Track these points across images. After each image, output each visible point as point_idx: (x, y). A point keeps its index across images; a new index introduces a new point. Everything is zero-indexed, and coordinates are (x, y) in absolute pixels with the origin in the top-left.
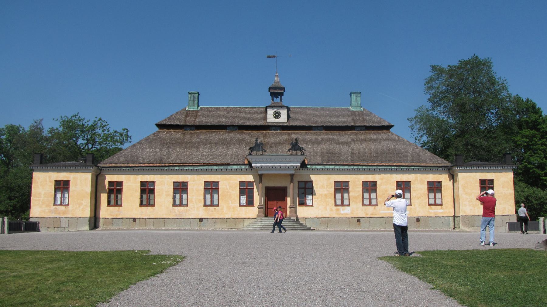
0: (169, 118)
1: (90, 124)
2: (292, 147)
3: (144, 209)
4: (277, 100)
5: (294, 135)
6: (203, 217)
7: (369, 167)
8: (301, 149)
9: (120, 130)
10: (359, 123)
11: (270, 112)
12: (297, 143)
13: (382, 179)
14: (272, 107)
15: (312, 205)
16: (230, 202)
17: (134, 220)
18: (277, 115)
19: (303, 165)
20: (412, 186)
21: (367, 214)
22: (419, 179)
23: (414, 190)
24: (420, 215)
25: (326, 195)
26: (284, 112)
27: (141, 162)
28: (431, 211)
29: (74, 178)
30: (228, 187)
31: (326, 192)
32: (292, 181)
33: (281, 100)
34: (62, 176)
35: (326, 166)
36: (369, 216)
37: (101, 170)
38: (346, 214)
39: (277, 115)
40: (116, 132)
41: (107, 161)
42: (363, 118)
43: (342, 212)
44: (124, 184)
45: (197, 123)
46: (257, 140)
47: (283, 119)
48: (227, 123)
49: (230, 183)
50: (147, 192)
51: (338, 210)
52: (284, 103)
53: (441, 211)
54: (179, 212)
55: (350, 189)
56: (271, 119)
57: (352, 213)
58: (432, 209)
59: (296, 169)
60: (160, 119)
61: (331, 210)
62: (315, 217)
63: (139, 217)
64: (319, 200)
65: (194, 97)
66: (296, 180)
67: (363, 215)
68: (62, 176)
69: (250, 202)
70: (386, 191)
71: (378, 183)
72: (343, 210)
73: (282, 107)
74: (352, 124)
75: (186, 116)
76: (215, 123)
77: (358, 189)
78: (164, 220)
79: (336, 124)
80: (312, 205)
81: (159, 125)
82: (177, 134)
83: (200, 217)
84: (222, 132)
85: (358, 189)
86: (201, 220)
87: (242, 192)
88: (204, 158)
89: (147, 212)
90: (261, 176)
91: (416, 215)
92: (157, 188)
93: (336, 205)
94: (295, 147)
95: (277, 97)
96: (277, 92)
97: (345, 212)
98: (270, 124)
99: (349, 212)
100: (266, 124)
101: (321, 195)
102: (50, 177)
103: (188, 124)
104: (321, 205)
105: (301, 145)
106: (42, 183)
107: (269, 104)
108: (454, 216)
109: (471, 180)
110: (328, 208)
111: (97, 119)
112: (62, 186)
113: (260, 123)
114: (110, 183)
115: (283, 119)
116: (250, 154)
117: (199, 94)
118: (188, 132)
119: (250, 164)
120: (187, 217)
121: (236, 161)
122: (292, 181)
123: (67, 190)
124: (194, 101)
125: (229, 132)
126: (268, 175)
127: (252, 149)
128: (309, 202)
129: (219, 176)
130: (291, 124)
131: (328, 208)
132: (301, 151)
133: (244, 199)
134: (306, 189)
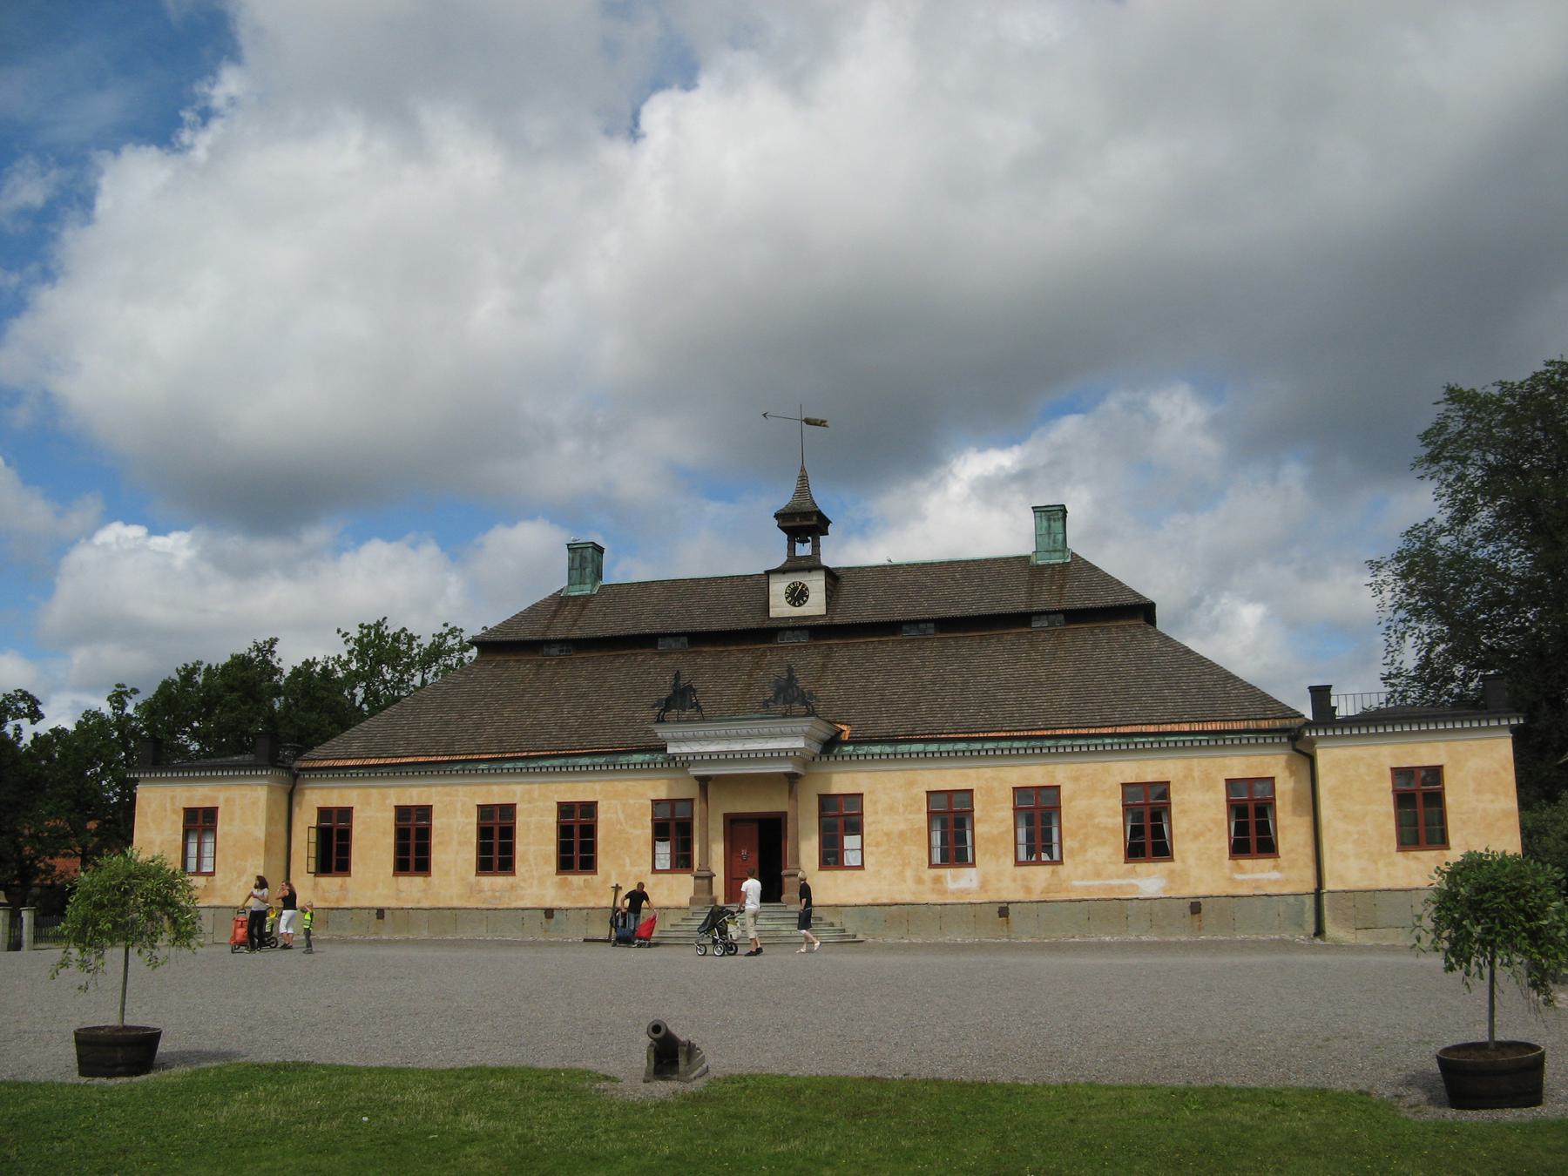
1: (427, 642)
2: (777, 695)
3: (405, 881)
4: (804, 550)
6: (555, 904)
7: (1033, 743)
10: (1046, 600)
11: (779, 588)
12: (791, 678)
13: (1076, 779)
14: (782, 571)
15: (862, 867)
16: (628, 861)
17: (380, 913)
18: (798, 595)
20: (1174, 797)
21: (1028, 890)
22: (1196, 774)
23: (1183, 812)
24: (1201, 891)
25: (902, 834)
26: (816, 585)
27: (400, 751)
28: (1239, 877)
29: (227, 800)
30: (622, 816)
31: (903, 826)
33: (816, 546)
35: (895, 739)
36: (1035, 898)
37: (296, 777)
38: (965, 891)
39: (798, 595)
41: (318, 751)
42: (1062, 587)
43: (951, 885)
44: (355, 815)
46: (677, 677)
47: (815, 605)
48: (658, 628)
49: (625, 805)
51: (937, 880)
53: (1275, 875)
54: (494, 891)
55: (976, 814)
56: (780, 607)
57: (983, 886)
58: (1241, 870)
61: (919, 881)
62: (870, 901)
63: (393, 904)
64: (882, 849)
65: (583, 558)
67: (1020, 896)
68: (199, 794)
69: (682, 861)
70: (1090, 816)
71: (1064, 793)
72: (955, 879)
74: (1022, 608)
76: (627, 628)
77: (1001, 814)
78: (452, 915)
79: (972, 611)
80: (862, 867)
82: (521, 669)
83: (548, 905)
85: (1001, 814)
86: (549, 913)
87: (660, 831)
88: (565, 735)
89: (412, 890)
91: (1189, 891)
92: (437, 823)
93: (931, 866)
95: (804, 541)
97: (961, 883)
98: (774, 625)
99: (975, 885)
100: (767, 624)
101: (887, 834)
102: (173, 798)
104: (887, 864)
108: (1318, 894)
109: (1363, 770)
110: (909, 873)
111: (446, 630)
112: (200, 821)
113: (750, 622)
114: (324, 813)
115: (815, 605)
116: (660, 720)
117: (600, 550)
120: (514, 905)
124: (582, 568)
125: (661, 654)
126: (719, 777)
127: (668, 704)
128: (851, 858)
129: (598, 786)
130: (838, 620)
131: (909, 873)
132: (805, 703)
133: (664, 849)
134: (841, 819)
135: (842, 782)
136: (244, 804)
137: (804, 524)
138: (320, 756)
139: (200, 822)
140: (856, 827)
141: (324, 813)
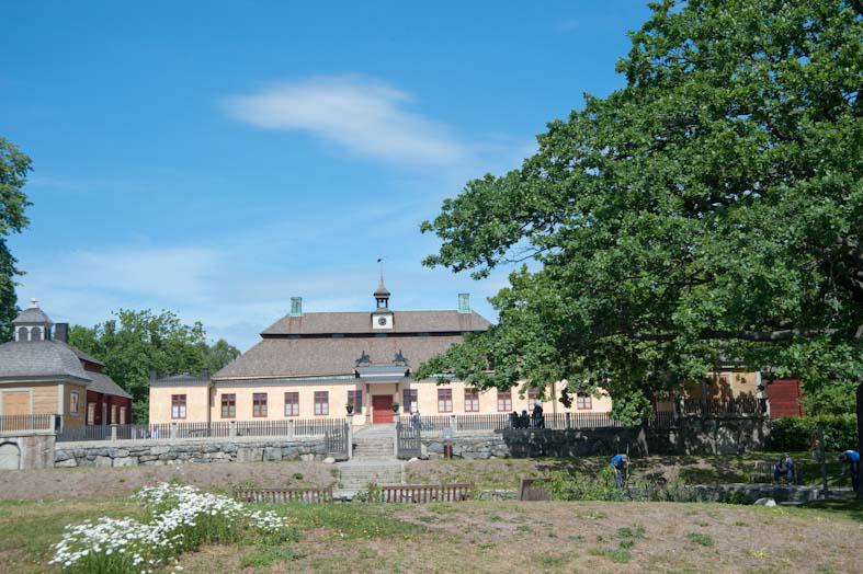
0: (272, 327)
4: (382, 305)
5: (401, 341)
8: (404, 360)
9: (192, 325)
12: (400, 355)
18: (383, 322)
19: (407, 374)
26: (389, 318)
32: (397, 390)
34: (179, 390)
39: (383, 322)
40: (187, 327)
41: (218, 373)
45: (302, 332)
47: (389, 326)
50: (260, 401)
52: (390, 309)
56: (376, 326)
59: (401, 378)
60: (265, 326)
66: (401, 388)
68: (179, 390)
73: (387, 313)
75: (290, 324)
76: (321, 331)
81: (262, 335)
84: (328, 340)
90: (368, 386)
94: (400, 358)
96: (382, 297)
103: (293, 332)
105: (404, 356)
106: (159, 399)
107: (374, 309)
112: (179, 400)
114: (224, 396)
118: (294, 341)
119: (357, 375)
121: (344, 371)
122: (397, 390)
123: (185, 403)
127: (360, 361)
130: (397, 331)
135: (413, 386)
136: (197, 394)
137: (382, 297)
138: (220, 375)
139: (179, 400)
140: (415, 399)
141: (224, 396)
